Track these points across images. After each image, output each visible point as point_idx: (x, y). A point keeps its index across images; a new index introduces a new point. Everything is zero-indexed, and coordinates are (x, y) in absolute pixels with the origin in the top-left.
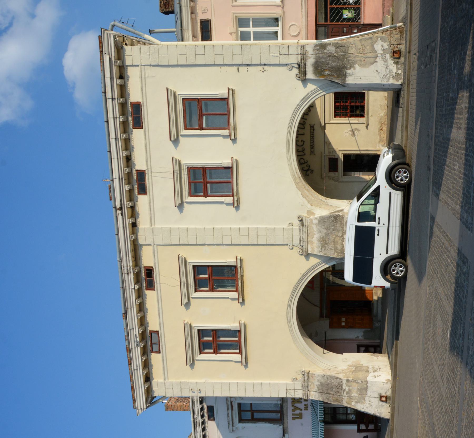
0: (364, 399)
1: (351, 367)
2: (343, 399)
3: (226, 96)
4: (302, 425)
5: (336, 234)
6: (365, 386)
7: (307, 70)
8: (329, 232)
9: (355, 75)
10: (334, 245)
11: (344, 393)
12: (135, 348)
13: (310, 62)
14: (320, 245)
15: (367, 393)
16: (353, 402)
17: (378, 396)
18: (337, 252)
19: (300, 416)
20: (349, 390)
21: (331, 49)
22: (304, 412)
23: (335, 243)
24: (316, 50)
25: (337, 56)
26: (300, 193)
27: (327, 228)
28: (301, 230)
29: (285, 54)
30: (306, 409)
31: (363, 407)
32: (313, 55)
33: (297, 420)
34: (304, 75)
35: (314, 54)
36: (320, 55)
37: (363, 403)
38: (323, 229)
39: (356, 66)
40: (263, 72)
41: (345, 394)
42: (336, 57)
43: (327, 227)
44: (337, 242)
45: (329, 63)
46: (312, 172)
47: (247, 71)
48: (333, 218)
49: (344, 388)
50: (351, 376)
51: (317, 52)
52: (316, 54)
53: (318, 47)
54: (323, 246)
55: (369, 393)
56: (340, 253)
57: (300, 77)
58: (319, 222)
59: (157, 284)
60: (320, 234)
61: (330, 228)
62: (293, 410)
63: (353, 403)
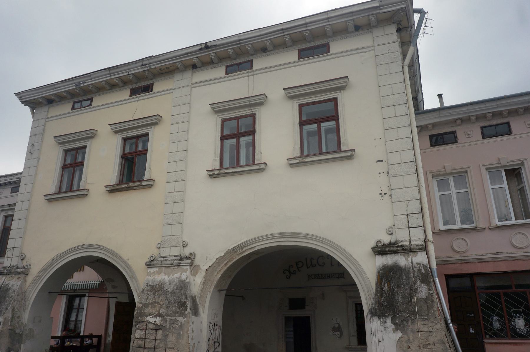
1: (23, 328)
3: (343, 148)
5: (164, 305)
7: (389, 256)
8: (168, 296)
9: (384, 332)
10: (152, 303)
12: (74, 83)
13: (402, 260)
14: (156, 283)
18: (142, 307)
21: (423, 291)
23: (153, 304)
24: (420, 267)
25: (413, 301)
26: (222, 254)
27: (173, 293)
28: (175, 258)
29: (408, 222)
32: (411, 264)
34: (380, 251)
35: (412, 265)
36: (412, 274)
38: (173, 288)
39: (399, 334)
40: (381, 194)
42: (411, 299)
43: (174, 293)
44: (154, 307)
45: (401, 288)
46: (288, 278)
47: (379, 173)
48: (184, 300)
50: (5, 328)
51: (416, 269)
52: (413, 269)
53: (423, 271)
54: (153, 288)
56: (141, 311)
57: (377, 246)
58: (183, 282)
59: (136, 97)
60: (168, 283)
61: (173, 297)
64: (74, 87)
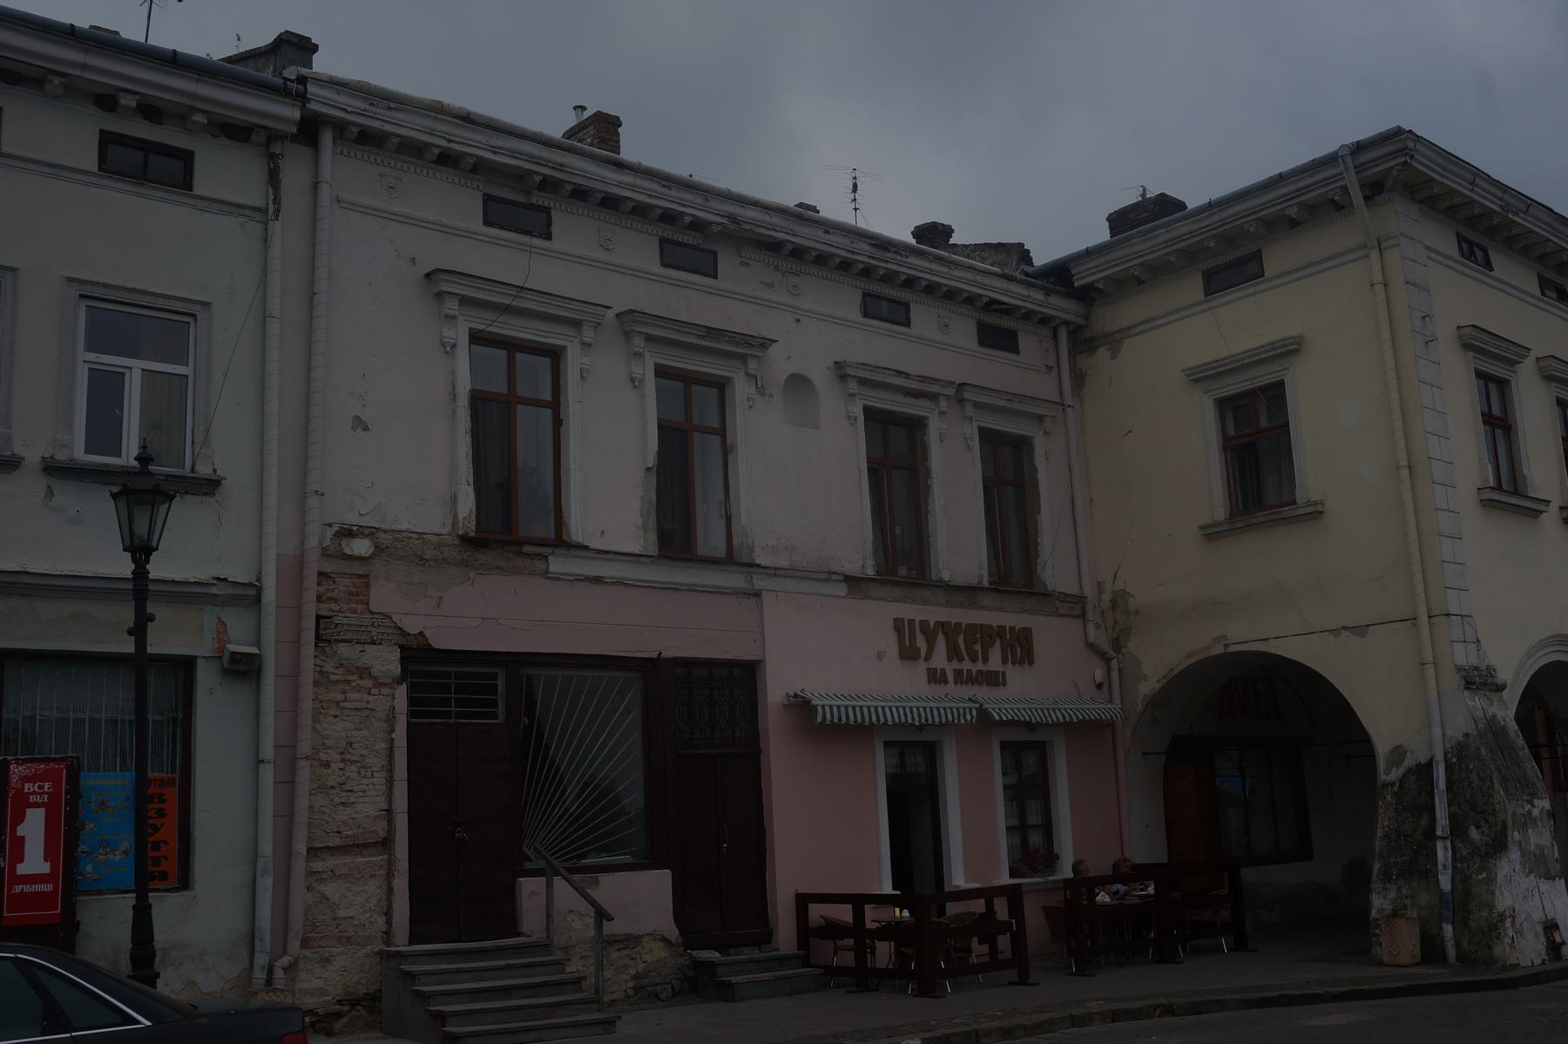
0: (1530, 872)
2: (1518, 801)
4: (880, 656)
6: (1553, 874)
11: (1528, 801)
15: (1542, 880)
16: (1519, 833)
17: (1549, 918)
19: (908, 654)
20: (1534, 820)
22: (922, 667)
30: (935, 677)
31: (1517, 871)
33: (894, 637)
37: (1523, 864)
41: (1528, 807)
49: (1536, 801)
55: (1545, 886)
62: (924, 624)
64: (1498, 209)
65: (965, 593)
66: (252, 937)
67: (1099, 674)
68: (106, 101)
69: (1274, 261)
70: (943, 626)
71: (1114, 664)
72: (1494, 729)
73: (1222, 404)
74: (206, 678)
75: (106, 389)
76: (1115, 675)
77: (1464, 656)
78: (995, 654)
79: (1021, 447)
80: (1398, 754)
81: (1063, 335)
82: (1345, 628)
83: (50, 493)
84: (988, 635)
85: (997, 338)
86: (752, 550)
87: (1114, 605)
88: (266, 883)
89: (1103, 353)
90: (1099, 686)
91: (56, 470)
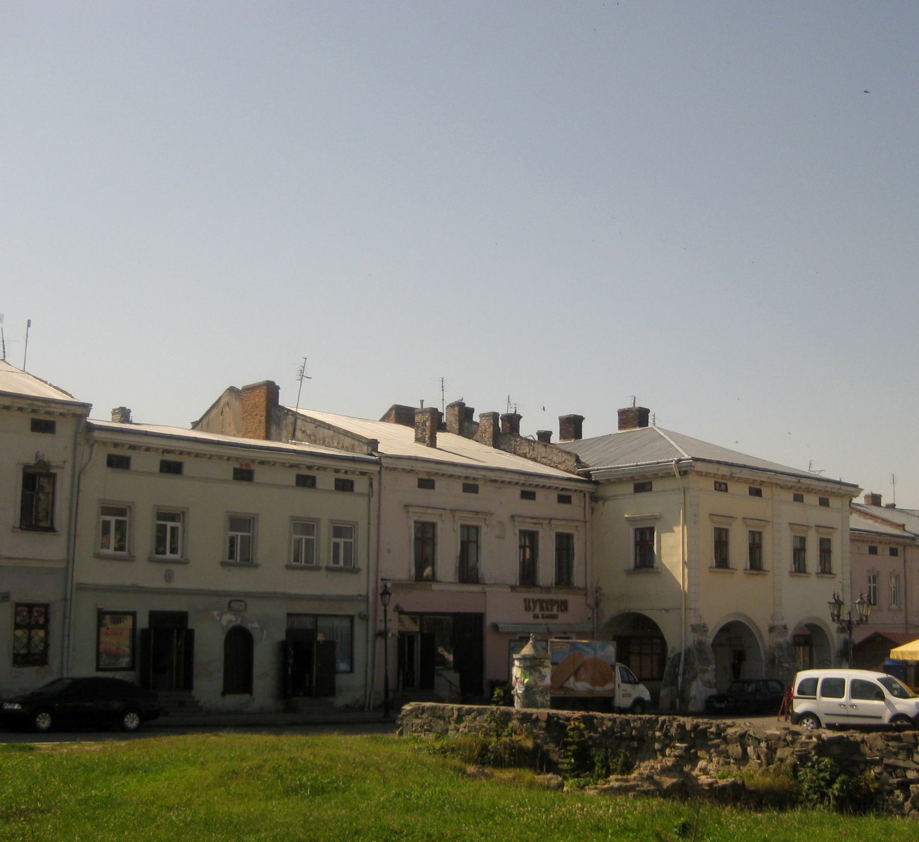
19: (527, 609)
41: (706, 667)
49: (710, 666)
62: (533, 600)
63: (700, 675)
65: (548, 589)
66: (366, 685)
67: (589, 616)
68: (337, 471)
69: (656, 486)
70: (539, 600)
71: (595, 611)
72: (700, 644)
73: (636, 530)
74: (357, 620)
75: (336, 545)
76: (595, 615)
77: (693, 621)
78: (555, 608)
79: (569, 537)
80: (674, 648)
81: (587, 495)
82: (663, 609)
83: (327, 575)
84: (552, 602)
85: (564, 499)
86: (484, 579)
87: (597, 591)
88: (369, 672)
89: (600, 503)
90: (590, 619)
91: (328, 569)
